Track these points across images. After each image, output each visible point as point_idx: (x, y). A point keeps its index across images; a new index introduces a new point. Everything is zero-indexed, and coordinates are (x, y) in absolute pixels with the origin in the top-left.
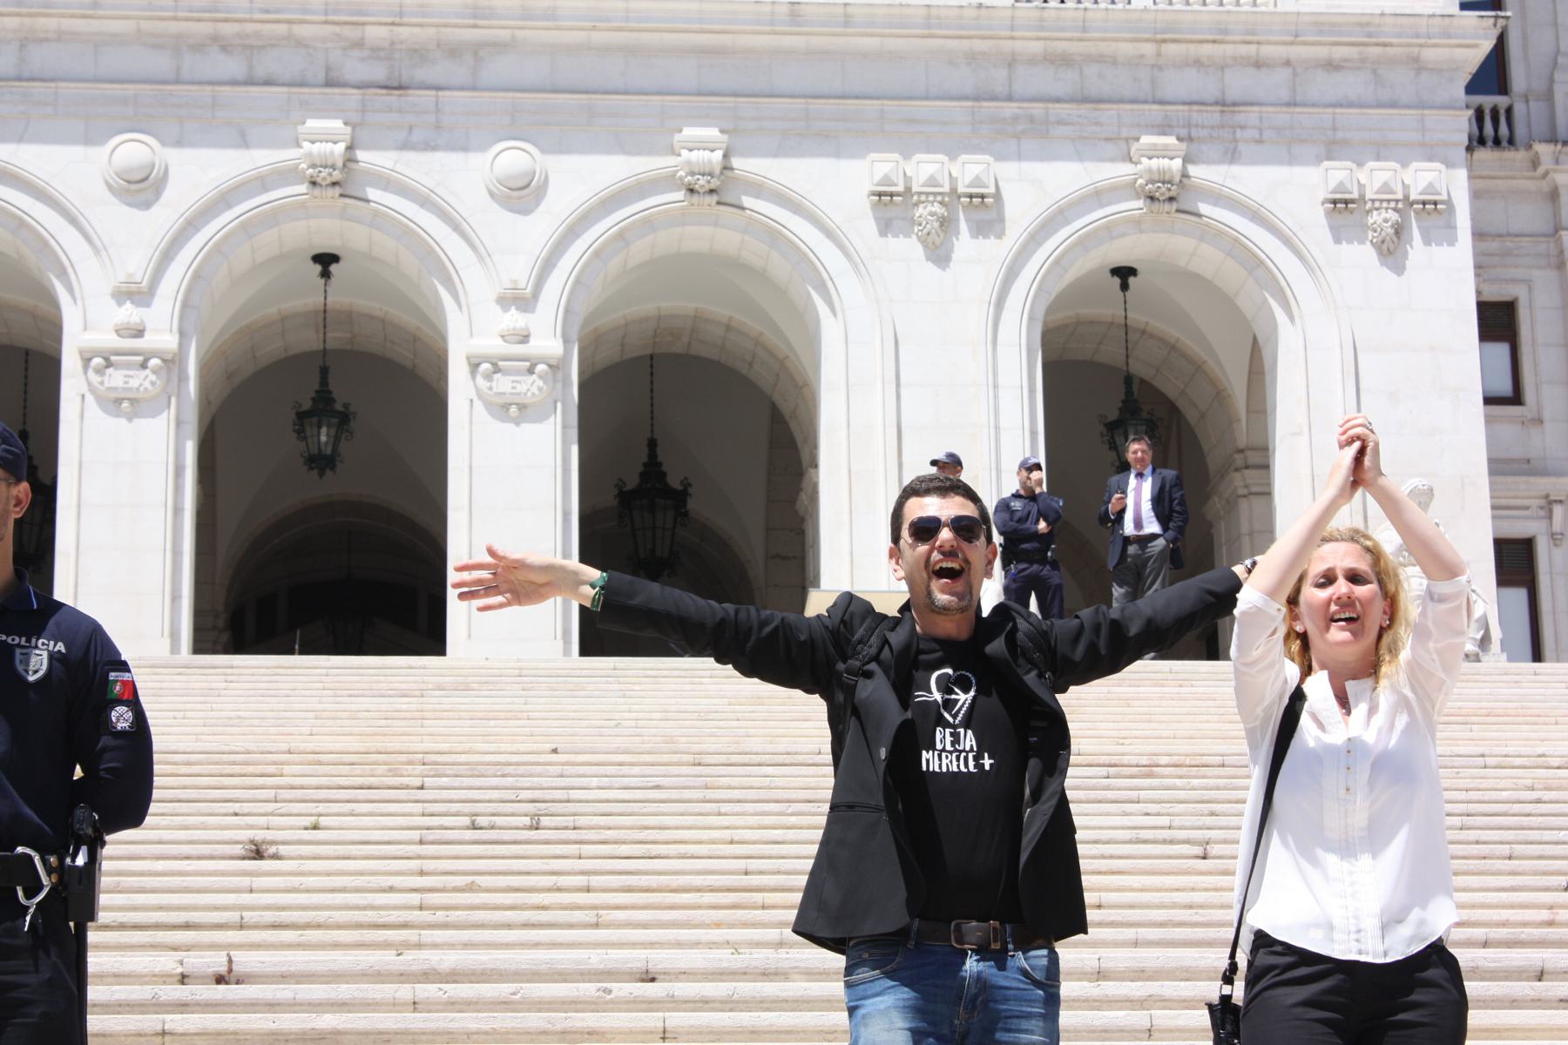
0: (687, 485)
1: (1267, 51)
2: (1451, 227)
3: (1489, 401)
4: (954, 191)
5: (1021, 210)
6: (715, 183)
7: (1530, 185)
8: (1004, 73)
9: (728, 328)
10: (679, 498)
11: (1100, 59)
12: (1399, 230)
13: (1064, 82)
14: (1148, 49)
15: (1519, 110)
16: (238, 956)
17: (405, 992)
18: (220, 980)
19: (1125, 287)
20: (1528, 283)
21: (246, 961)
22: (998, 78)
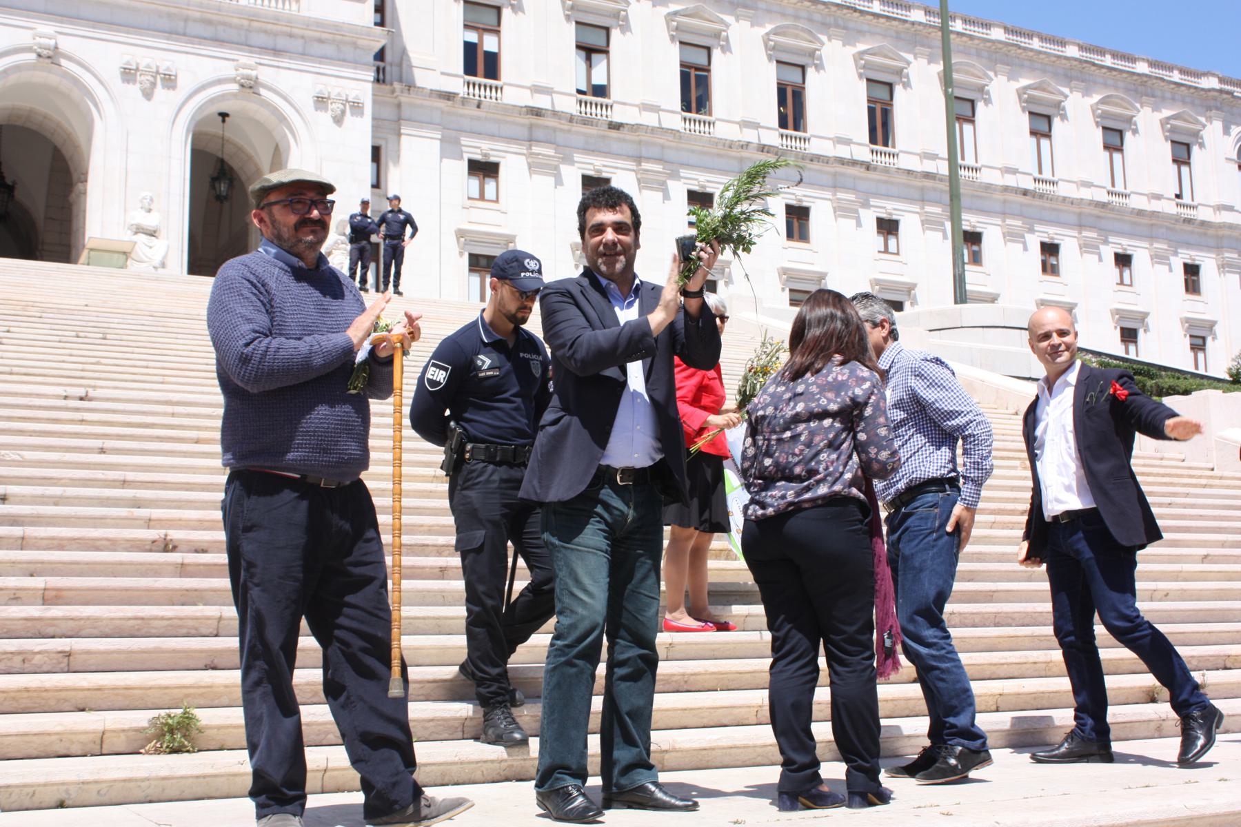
0: (14, 183)
1: (295, 31)
2: (362, 114)
3: (373, 186)
4: (157, 72)
5: (186, 83)
6: (51, 53)
7: (391, 100)
8: (181, 24)
9: (45, 117)
10: (10, 189)
11: (224, 24)
12: (343, 112)
13: (209, 31)
14: (246, 23)
15: (388, 69)
16: (90, 390)
17: (169, 409)
18: (81, 399)
19: (224, 121)
20: (386, 140)
21: (92, 393)
22: (180, 26)
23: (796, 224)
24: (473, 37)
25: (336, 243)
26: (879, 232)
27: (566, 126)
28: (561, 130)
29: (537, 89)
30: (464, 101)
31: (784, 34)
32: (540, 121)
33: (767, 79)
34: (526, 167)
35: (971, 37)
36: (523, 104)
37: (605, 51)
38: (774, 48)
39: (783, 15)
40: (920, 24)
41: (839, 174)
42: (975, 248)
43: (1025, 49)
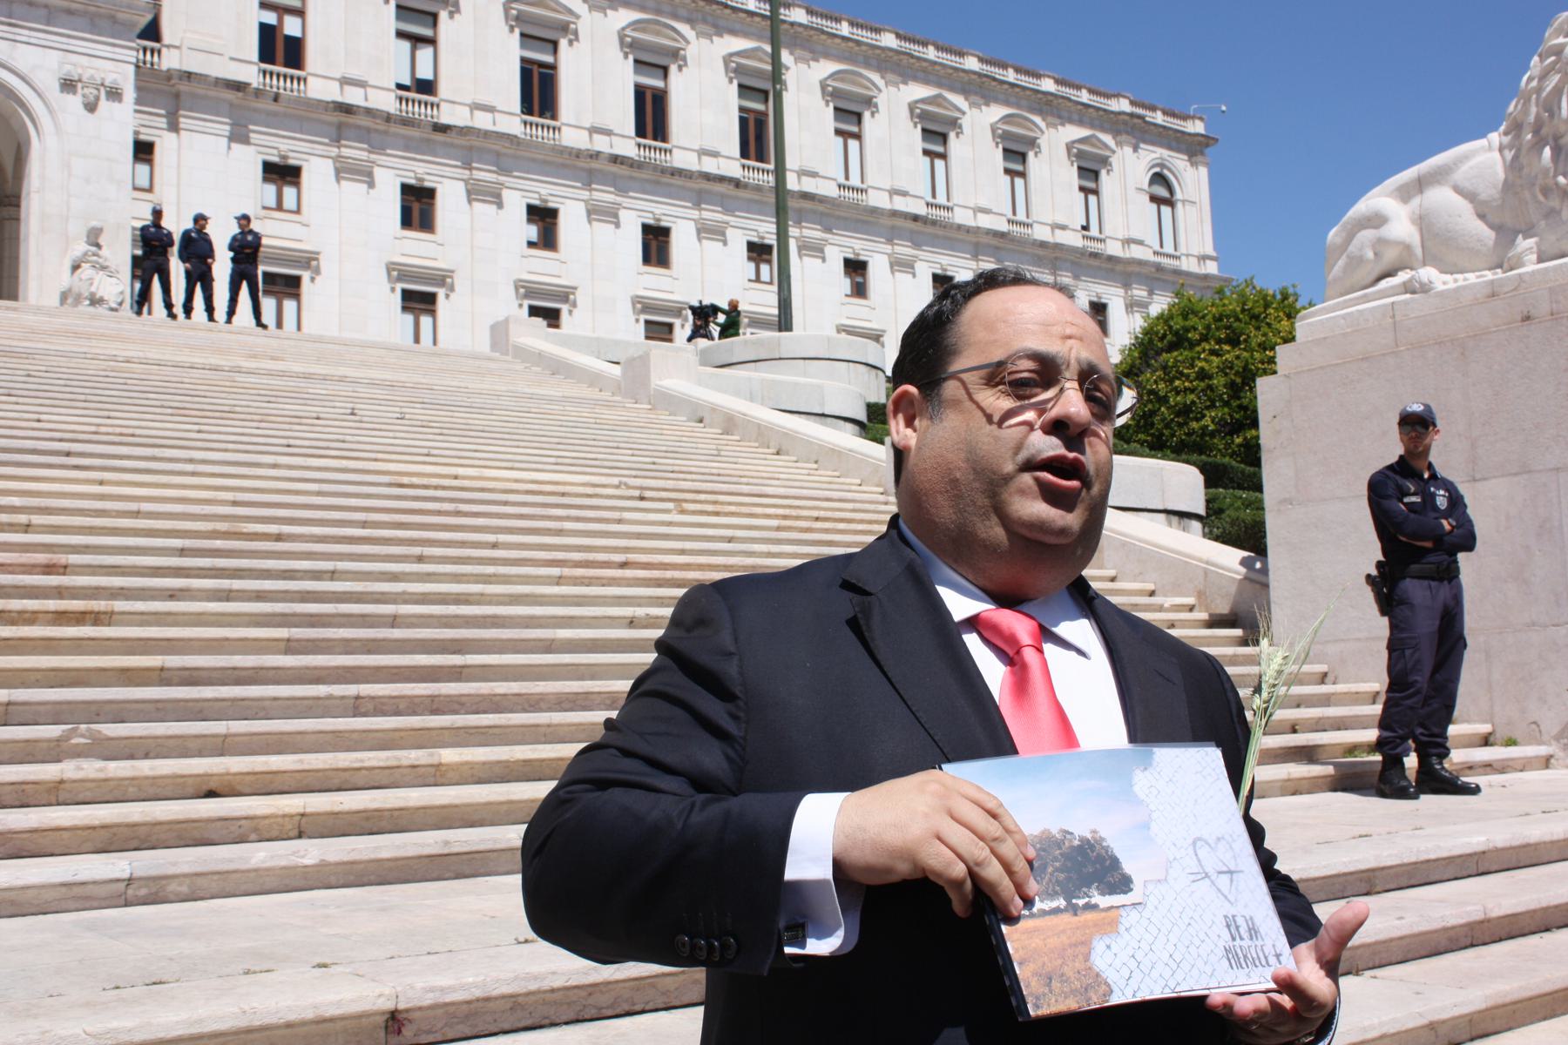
12: (97, 98)
23: (654, 244)
24: (270, 18)
25: (86, 254)
26: (750, 259)
27: (382, 127)
28: (376, 131)
29: (345, 81)
30: (258, 93)
31: (644, 30)
32: (351, 119)
33: (623, 78)
34: (332, 172)
35: (858, 43)
36: (329, 99)
37: (432, 41)
38: (631, 46)
39: (643, 9)
40: (800, 25)
41: (702, 188)
42: (859, 279)
43: (919, 59)
